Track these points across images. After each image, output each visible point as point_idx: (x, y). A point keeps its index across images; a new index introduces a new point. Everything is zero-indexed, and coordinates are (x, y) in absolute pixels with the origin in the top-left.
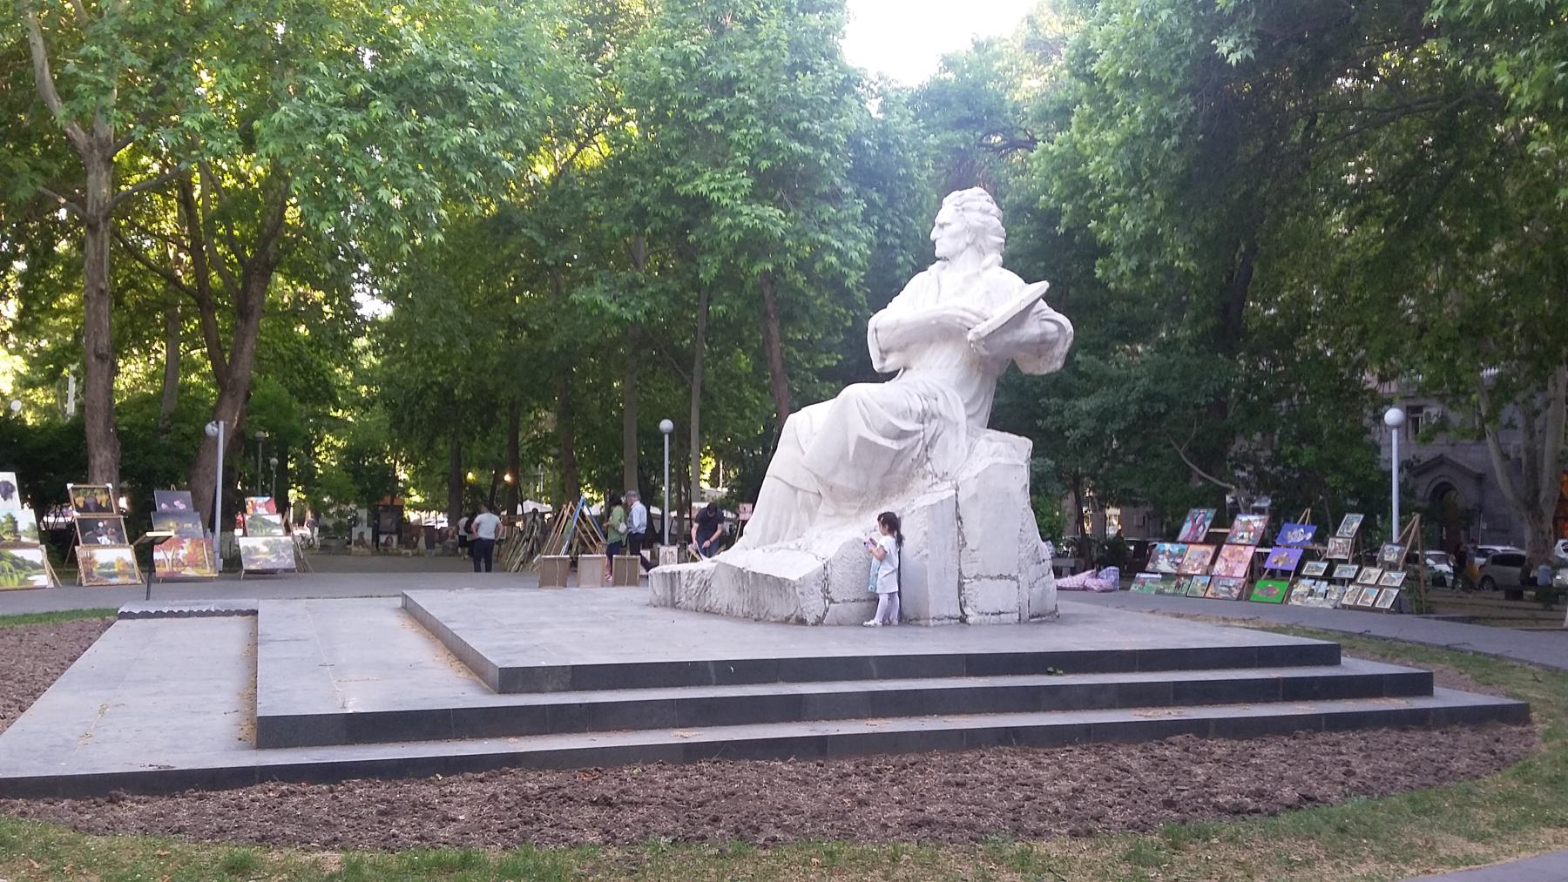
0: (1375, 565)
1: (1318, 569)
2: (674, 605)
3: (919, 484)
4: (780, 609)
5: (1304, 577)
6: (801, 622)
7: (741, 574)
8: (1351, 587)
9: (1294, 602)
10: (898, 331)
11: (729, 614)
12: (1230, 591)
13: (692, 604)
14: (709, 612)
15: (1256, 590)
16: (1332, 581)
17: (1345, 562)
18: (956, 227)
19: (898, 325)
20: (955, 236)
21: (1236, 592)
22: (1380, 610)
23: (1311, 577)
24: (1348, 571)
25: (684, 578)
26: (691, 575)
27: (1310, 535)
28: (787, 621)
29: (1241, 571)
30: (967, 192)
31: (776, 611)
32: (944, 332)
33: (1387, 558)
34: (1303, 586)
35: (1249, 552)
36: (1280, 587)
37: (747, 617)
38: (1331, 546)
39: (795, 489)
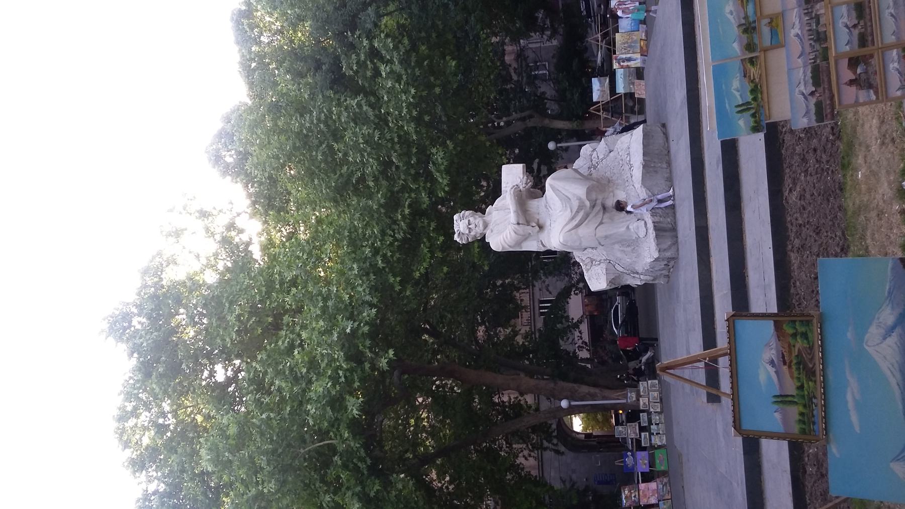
0: (639, 406)
1: (645, 437)
2: (674, 229)
3: (594, 176)
4: (659, 139)
5: (651, 444)
6: (664, 125)
7: (646, 166)
8: (652, 410)
9: (664, 442)
12: (666, 484)
15: (663, 468)
16: (650, 423)
17: (640, 423)
18: (471, 219)
20: (475, 219)
21: (665, 480)
22: (661, 399)
23: (650, 440)
24: (644, 417)
25: (657, 219)
27: (629, 453)
28: (666, 135)
29: (653, 485)
33: (634, 399)
34: (656, 441)
35: (642, 486)
36: (658, 454)
37: (669, 164)
38: (633, 436)
39: (601, 223)
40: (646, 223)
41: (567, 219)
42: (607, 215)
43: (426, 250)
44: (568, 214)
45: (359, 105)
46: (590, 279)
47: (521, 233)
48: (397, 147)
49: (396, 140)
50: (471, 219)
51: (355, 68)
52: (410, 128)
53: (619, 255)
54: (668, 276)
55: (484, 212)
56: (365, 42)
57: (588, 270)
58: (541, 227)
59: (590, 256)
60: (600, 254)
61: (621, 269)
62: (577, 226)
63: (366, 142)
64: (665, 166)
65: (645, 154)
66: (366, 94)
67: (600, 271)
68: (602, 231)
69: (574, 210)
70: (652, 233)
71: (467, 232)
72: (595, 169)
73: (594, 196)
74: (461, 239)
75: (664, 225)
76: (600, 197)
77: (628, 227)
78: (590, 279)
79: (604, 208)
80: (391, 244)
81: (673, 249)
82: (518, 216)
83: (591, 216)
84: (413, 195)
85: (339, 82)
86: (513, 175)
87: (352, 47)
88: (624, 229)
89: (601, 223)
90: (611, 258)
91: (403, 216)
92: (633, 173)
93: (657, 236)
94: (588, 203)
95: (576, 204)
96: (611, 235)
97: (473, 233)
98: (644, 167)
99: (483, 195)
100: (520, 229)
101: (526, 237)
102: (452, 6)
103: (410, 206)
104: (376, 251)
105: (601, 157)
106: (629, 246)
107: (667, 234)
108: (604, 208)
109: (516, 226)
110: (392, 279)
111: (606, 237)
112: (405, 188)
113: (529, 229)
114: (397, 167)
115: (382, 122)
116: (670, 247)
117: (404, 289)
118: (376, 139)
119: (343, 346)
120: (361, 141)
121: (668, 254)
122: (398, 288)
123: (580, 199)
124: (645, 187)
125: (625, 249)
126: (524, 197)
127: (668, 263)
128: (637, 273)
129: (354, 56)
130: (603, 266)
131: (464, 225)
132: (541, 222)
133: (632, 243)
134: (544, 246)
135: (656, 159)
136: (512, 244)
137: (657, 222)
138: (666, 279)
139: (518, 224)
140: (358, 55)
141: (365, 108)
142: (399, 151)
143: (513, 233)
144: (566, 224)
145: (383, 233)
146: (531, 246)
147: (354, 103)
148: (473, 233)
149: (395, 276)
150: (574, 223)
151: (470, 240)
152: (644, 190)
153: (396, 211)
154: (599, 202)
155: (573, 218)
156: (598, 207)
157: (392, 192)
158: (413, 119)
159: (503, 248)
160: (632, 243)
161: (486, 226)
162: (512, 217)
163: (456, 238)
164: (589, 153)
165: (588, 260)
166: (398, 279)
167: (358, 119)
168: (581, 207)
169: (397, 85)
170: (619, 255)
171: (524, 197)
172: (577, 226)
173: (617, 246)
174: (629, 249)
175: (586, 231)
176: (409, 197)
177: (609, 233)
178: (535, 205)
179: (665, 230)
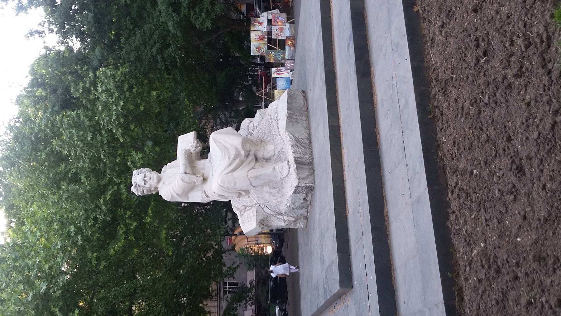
2: (311, 164)
4: (300, 100)
7: (290, 117)
10: (188, 166)
11: (308, 128)
13: (308, 151)
14: (310, 139)
18: (147, 174)
19: (185, 164)
25: (297, 155)
26: (294, 153)
28: (306, 98)
30: (134, 173)
31: (302, 102)
32: (191, 160)
37: (308, 117)
40: (288, 162)
41: (226, 165)
42: (258, 164)
43: (121, 232)
44: (226, 162)
45: (78, 116)
46: (243, 222)
47: (188, 180)
48: (106, 147)
49: (105, 142)
50: (147, 174)
51: (81, 91)
52: (118, 133)
53: (267, 196)
54: (306, 218)
55: (160, 171)
56: (91, 75)
57: (242, 216)
58: (205, 180)
59: (245, 204)
60: (251, 200)
61: (268, 211)
62: (233, 170)
63: (82, 141)
64: (304, 118)
65: (288, 109)
66: (86, 109)
67: (252, 214)
68: (253, 173)
69: (232, 157)
70: (293, 166)
71: (142, 184)
72: (251, 135)
73: (248, 147)
74: (137, 190)
75: (304, 160)
76: (253, 149)
77: (274, 168)
78: (243, 222)
79: (257, 159)
80: (93, 225)
81: (310, 177)
82: (186, 167)
83: (245, 164)
84: (116, 188)
85: (67, 103)
86: (187, 142)
87: (81, 78)
88: (271, 169)
89: (253, 168)
90: (262, 202)
91: (105, 201)
92: (278, 125)
93: (297, 168)
94: (243, 153)
95: (233, 153)
96: (260, 175)
97: (147, 186)
98: (288, 117)
99: (160, 158)
100: (187, 177)
101: (192, 187)
102: (159, 57)
103: (111, 195)
104: (80, 230)
105: (255, 125)
106: (275, 188)
107: (306, 167)
108: (257, 159)
109: (184, 175)
110: (90, 255)
111: (256, 177)
112: (111, 181)
113: (194, 178)
114: (105, 164)
115: (96, 129)
116: (307, 177)
117: (99, 264)
118: (89, 138)
119: (37, 305)
120: (76, 138)
121: (306, 183)
122: (94, 263)
123: (236, 149)
124: (288, 131)
125: (272, 190)
126: (194, 158)
127: (306, 191)
128: (282, 214)
129: (81, 84)
130: (254, 209)
131: (141, 180)
132: (205, 175)
133: (276, 185)
134: (207, 196)
135: (298, 113)
136: (179, 192)
137: (298, 158)
138: (305, 221)
139: (185, 173)
140: (85, 84)
141: (82, 118)
142: (107, 151)
143: (180, 182)
144: (224, 170)
145: (87, 218)
146: (196, 197)
147: (74, 114)
148: (147, 186)
149: (93, 252)
150: (231, 168)
151: (146, 193)
152: (287, 134)
153: (100, 198)
154: (252, 153)
155: (230, 165)
156: (251, 157)
157: (99, 186)
158: (120, 125)
159: (172, 196)
160: (276, 185)
161: (159, 180)
162: (181, 169)
163: (133, 189)
164: (247, 125)
165: (244, 207)
166: (95, 254)
167: (78, 125)
168: (237, 155)
169: (110, 100)
170: (267, 196)
171: (194, 158)
172: (233, 170)
173: (265, 189)
174: (275, 191)
175: (241, 173)
176: (112, 188)
177: (259, 173)
178: (202, 164)
179: (304, 164)
